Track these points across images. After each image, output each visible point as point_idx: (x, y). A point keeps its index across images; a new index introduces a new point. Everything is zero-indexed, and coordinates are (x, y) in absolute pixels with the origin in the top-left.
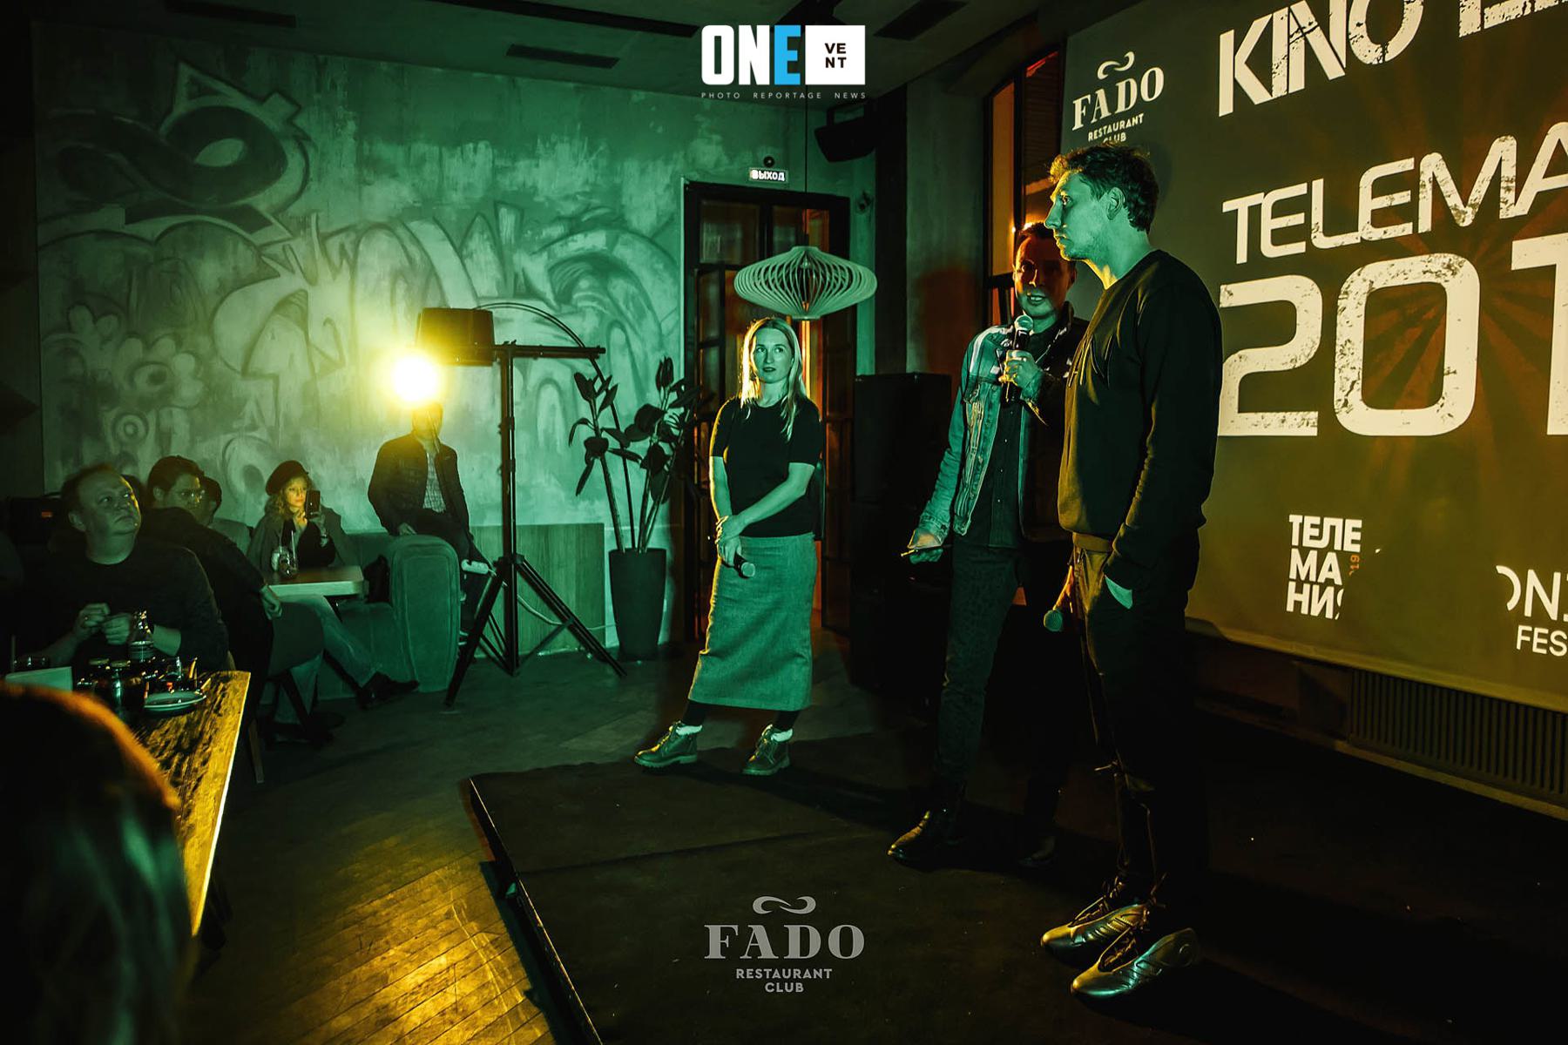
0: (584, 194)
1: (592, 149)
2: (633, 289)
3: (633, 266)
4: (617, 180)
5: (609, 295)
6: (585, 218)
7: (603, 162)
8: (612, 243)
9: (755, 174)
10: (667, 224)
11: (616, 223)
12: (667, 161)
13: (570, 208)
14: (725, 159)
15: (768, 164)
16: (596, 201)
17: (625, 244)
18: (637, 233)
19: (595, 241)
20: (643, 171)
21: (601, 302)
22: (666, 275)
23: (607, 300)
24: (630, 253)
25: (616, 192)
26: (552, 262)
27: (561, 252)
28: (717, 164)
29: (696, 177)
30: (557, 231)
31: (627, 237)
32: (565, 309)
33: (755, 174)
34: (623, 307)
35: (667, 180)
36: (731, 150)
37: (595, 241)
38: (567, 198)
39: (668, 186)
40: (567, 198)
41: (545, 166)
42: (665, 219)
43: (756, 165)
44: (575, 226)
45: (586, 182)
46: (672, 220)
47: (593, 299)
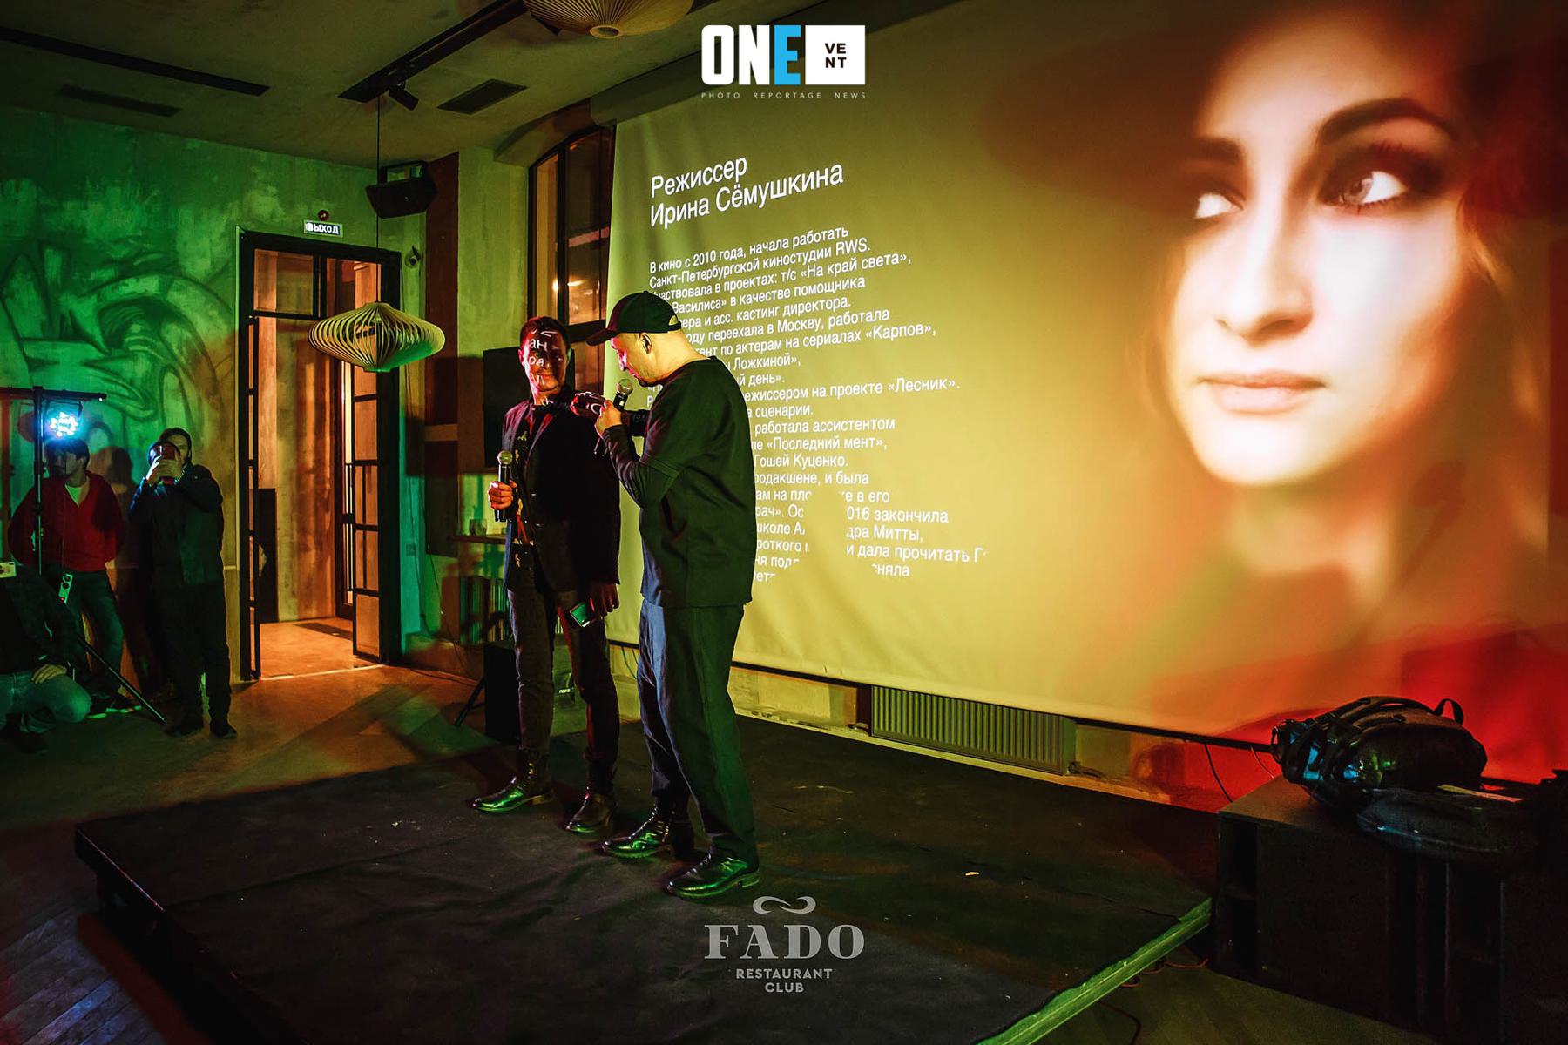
0: (137, 238)
1: (145, 193)
2: (187, 334)
3: (187, 312)
4: (171, 226)
5: (163, 340)
6: (137, 262)
7: (157, 208)
8: (165, 288)
9: (309, 227)
10: (222, 272)
11: (170, 268)
12: (222, 210)
13: (121, 252)
14: (280, 211)
15: (322, 217)
16: (147, 246)
17: (179, 290)
18: (192, 281)
19: (149, 285)
20: (197, 219)
21: (153, 347)
22: (220, 322)
23: (160, 344)
24: (184, 299)
25: (170, 238)
26: (103, 305)
27: (111, 295)
28: (273, 215)
29: (252, 227)
30: (107, 274)
31: (179, 282)
32: (116, 352)
33: (309, 227)
34: (176, 352)
35: (222, 229)
36: (289, 203)
37: (149, 285)
38: (117, 242)
39: (223, 235)
40: (117, 242)
41: (95, 208)
42: (220, 267)
43: (310, 218)
44: (127, 270)
45: (138, 227)
46: (226, 269)
47: (145, 343)
